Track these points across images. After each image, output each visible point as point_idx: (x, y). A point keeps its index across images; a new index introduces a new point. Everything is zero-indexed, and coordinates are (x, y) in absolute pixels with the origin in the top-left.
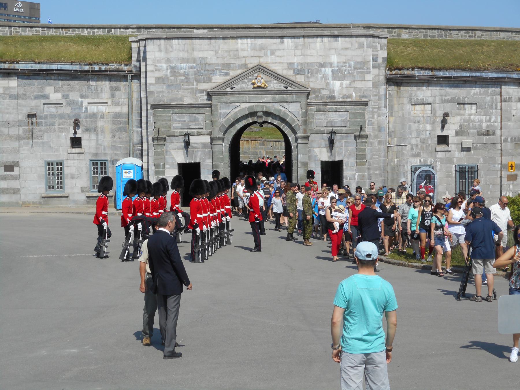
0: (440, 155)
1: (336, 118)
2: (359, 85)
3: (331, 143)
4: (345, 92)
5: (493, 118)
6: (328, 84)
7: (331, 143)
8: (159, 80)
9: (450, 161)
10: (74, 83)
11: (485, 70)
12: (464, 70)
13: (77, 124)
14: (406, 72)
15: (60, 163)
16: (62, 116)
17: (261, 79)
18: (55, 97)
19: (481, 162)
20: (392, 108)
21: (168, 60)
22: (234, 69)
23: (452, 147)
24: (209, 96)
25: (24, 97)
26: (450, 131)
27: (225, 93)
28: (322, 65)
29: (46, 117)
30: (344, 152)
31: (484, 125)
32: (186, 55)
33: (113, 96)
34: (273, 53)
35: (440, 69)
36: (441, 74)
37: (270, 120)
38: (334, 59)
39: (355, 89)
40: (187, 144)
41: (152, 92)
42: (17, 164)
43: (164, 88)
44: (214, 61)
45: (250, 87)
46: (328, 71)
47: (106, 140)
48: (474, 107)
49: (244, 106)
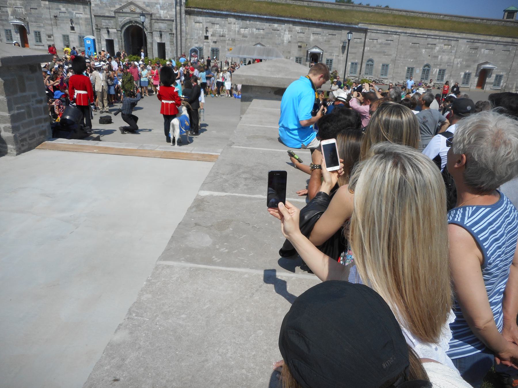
0: (205, 43)
1: (162, 26)
2: (170, 13)
3: (161, 35)
4: (165, 15)
6: (158, 12)
7: (161, 35)
8: (96, 5)
9: (209, 46)
11: (222, 11)
12: (214, 10)
13: (72, 22)
14: (192, 9)
15: (68, 36)
16: (66, 17)
17: (133, 7)
18: (63, 9)
19: (220, 47)
20: (187, 23)
23: (209, 40)
24: (115, 12)
25: (52, 8)
26: (209, 34)
27: (120, 12)
28: (156, 4)
29: (61, 17)
30: (166, 40)
31: (221, 33)
33: (84, 11)
35: (205, 9)
39: (169, 14)
41: (93, 10)
42: (52, 35)
43: (98, 8)
45: (129, 11)
46: (158, 6)
47: (83, 28)
49: (127, 18)
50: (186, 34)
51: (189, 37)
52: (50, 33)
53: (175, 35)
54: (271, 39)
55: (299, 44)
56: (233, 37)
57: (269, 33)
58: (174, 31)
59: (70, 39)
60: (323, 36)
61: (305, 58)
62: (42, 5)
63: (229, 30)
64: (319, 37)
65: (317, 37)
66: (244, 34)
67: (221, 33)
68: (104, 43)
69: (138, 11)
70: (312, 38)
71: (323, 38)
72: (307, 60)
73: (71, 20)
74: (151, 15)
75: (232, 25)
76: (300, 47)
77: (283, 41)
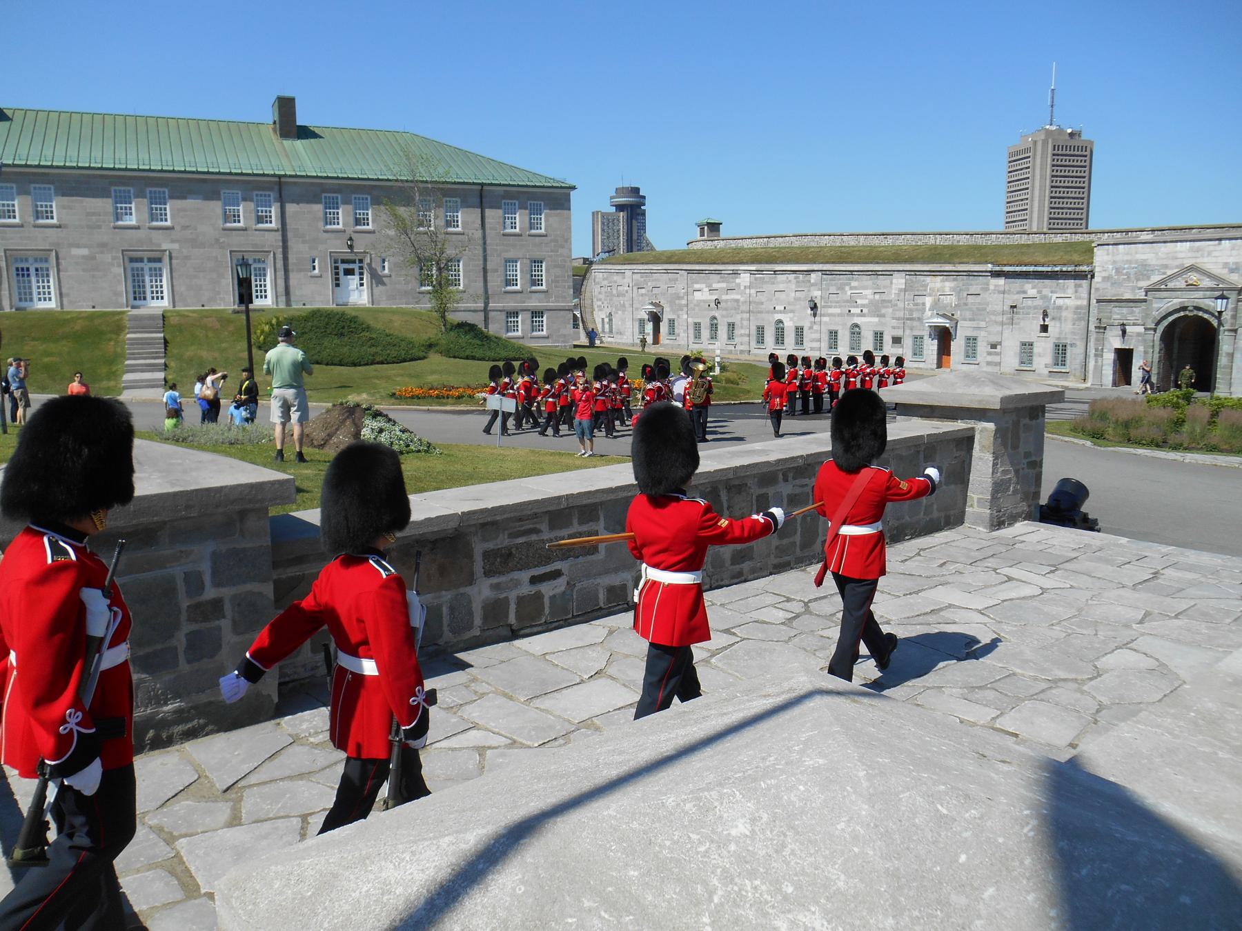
10: (1047, 282)
13: (1045, 315)
16: (1035, 308)
17: (1193, 277)
21: (1114, 262)
22: (1171, 268)
24: (1147, 291)
27: (1159, 290)
32: (1129, 258)
34: (1209, 254)
37: (1200, 314)
40: (1124, 332)
42: (1000, 343)
44: (1154, 262)
47: (1068, 327)
52: (994, 339)
59: (1036, 350)
62: (992, 287)
68: (1110, 357)
69: (1207, 283)
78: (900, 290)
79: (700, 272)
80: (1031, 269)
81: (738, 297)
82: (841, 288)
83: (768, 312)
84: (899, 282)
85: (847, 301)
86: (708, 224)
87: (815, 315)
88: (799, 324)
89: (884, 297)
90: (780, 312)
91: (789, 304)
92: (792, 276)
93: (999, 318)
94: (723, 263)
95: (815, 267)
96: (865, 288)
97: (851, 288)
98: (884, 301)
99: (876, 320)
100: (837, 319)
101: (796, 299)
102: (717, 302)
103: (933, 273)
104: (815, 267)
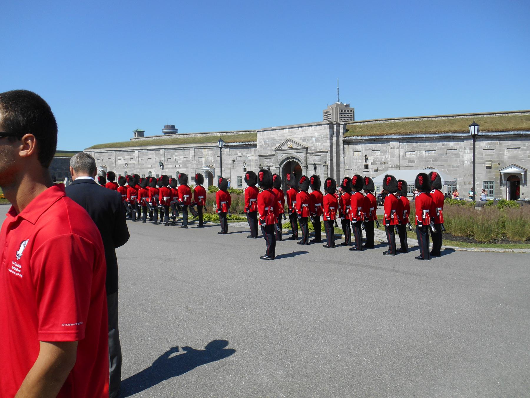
1: (317, 158)
2: (325, 144)
3: (315, 168)
5: (387, 157)
6: (314, 145)
7: (315, 168)
12: (374, 136)
16: (241, 161)
17: (290, 144)
21: (263, 139)
26: (369, 163)
27: (279, 150)
31: (383, 160)
34: (295, 134)
36: (364, 138)
38: (316, 134)
44: (277, 138)
45: (287, 148)
48: (379, 152)
49: (285, 155)
50: (344, 164)
51: (347, 168)
53: (329, 167)
54: (446, 161)
55: (488, 164)
56: (397, 163)
57: (443, 155)
58: (329, 163)
60: (523, 150)
61: (499, 181)
62: (225, 153)
63: (393, 156)
64: (519, 152)
65: (514, 152)
66: (410, 158)
67: (383, 160)
69: (295, 146)
70: (507, 154)
71: (525, 153)
72: (501, 184)
73: (244, 162)
74: (307, 149)
75: (395, 150)
76: (489, 167)
77: (463, 162)
78: (193, 156)
79: (120, 151)
80: (238, 144)
81: (134, 162)
82: (172, 156)
83: (146, 168)
84: (192, 152)
85: (174, 162)
86: (137, 131)
87: (163, 169)
88: (157, 173)
89: (188, 159)
90: (150, 168)
91: (154, 164)
92: (154, 152)
93: (229, 166)
94: (128, 147)
95: (162, 147)
96: (180, 155)
97: (176, 156)
98: (187, 161)
99: (185, 169)
100: (171, 170)
101: (156, 162)
102: (127, 165)
103: (204, 147)
104: (162, 147)
